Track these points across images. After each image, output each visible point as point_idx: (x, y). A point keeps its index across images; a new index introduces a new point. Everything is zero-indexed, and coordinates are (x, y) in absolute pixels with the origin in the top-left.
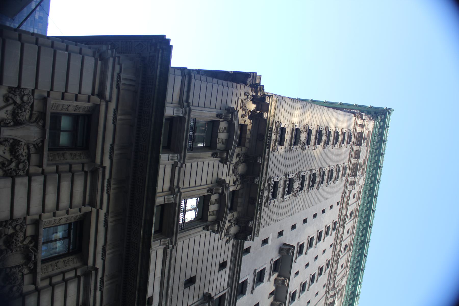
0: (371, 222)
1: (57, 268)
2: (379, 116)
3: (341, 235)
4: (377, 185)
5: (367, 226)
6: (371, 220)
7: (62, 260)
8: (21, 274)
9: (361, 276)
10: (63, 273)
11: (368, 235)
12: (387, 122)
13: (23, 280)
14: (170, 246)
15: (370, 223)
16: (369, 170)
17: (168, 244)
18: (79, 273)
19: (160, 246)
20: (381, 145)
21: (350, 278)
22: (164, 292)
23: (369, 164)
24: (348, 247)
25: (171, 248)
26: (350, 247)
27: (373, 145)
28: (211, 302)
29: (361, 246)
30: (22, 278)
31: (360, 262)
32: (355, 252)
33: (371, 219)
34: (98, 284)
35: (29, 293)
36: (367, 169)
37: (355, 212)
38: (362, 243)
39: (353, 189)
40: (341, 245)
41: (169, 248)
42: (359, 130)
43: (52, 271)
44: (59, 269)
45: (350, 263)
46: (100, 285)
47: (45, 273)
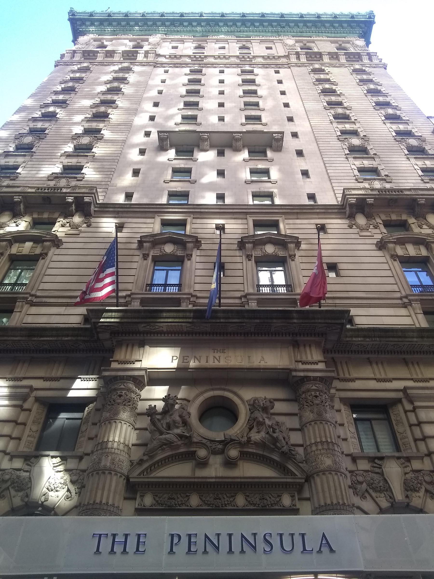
0: (216, 17)
2: (79, 28)
3: (215, 59)
4: (167, 16)
5: (221, 21)
6: (214, 16)
9: (291, 17)
11: (234, 17)
12: (85, 16)
15: (217, 17)
16: (147, 31)
20: (115, 20)
21: (294, 32)
23: (140, 33)
24: (244, 43)
26: (246, 42)
27: (115, 31)
28: (144, 240)
29: (249, 24)
31: (270, 22)
32: (256, 31)
33: (212, 16)
36: (146, 34)
37: (197, 42)
38: (246, 23)
39: (154, 52)
40: (230, 56)
42: (78, 57)
45: (271, 36)
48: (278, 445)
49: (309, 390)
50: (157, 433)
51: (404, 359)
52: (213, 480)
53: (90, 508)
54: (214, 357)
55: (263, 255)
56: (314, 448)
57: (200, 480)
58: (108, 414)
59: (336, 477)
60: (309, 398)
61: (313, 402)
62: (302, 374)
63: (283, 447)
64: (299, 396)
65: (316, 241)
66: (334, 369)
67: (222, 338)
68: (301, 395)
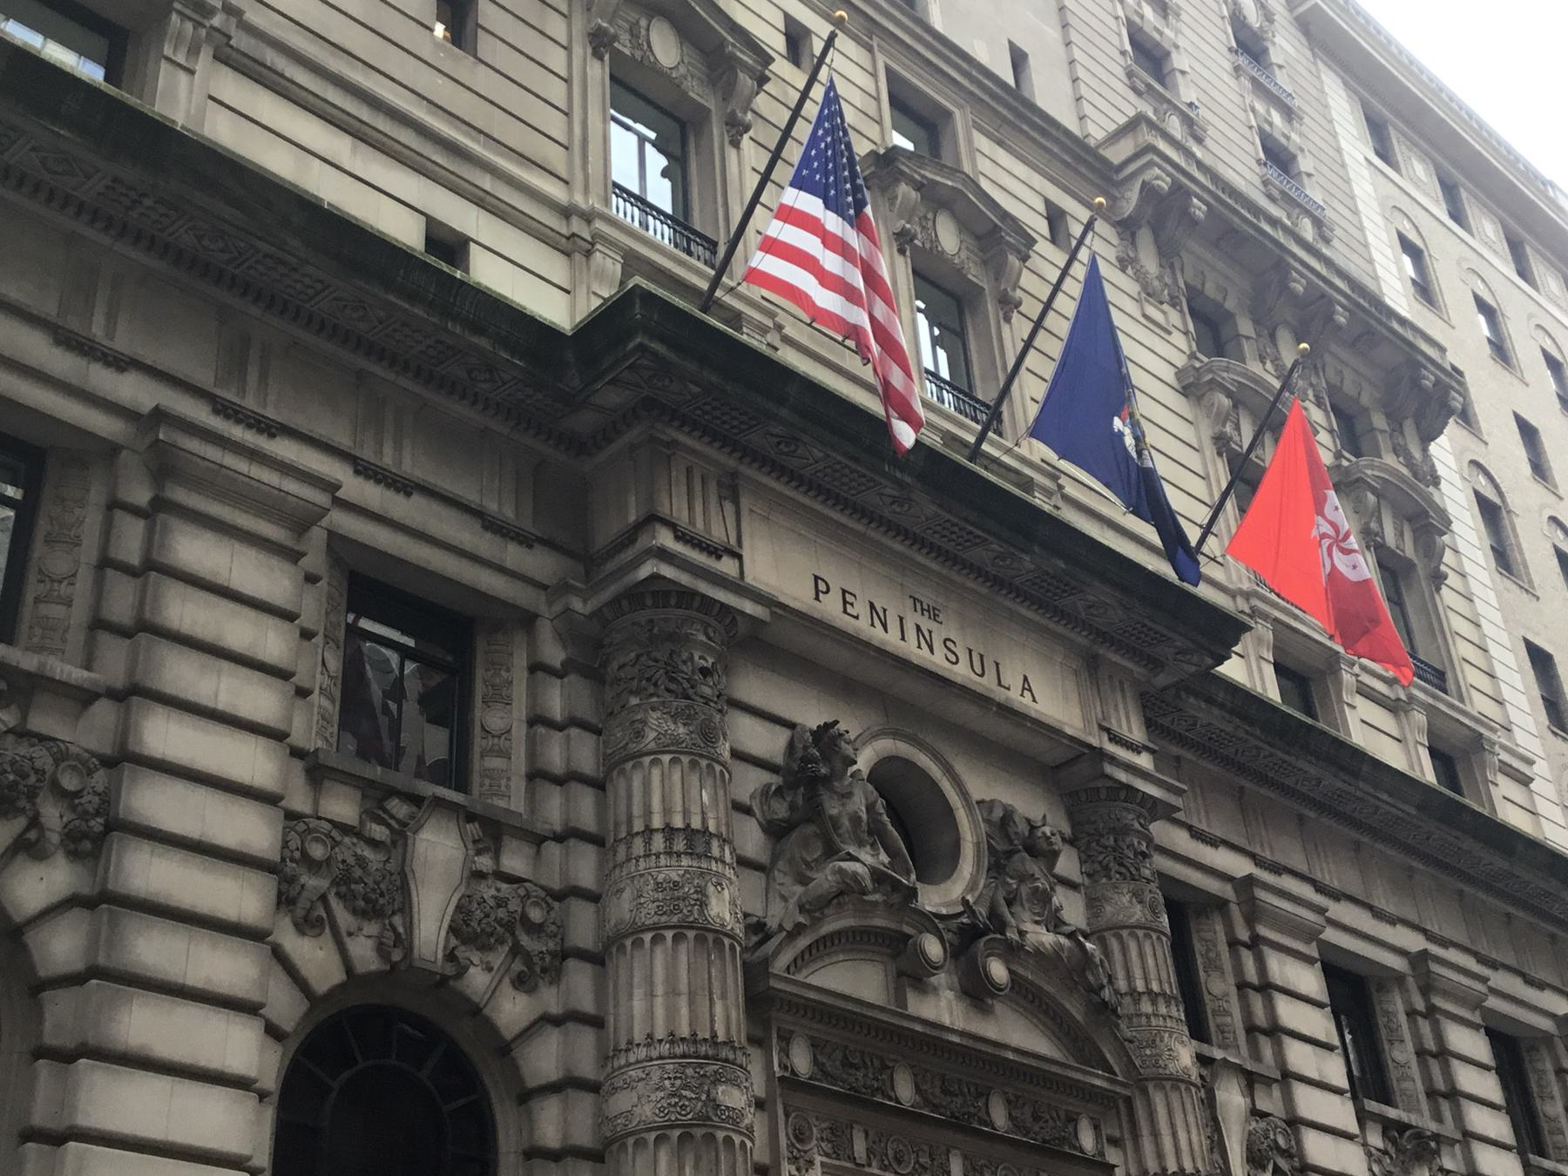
1: (66, 582)
7: (39, 549)
8: (11, 738)
10: (106, 563)
13: (43, 738)
14: (217, 21)
17: (203, 32)
18: (141, 495)
19: (191, 72)
22: (434, 158)
25: (233, 21)
30: (35, 740)
34: (238, 433)
35: (125, 730)
41: (224, 30)
43: (70, 606)
44: (74, 575)
46: (250, 426)
47: (64, 641)
48: (1091, 978)
49: (1126, 830)
50: (819, 844)
51: (1242, 789)
52: (956, 1039)
53: (710, 1053)
54: (918, 629)
55: (928, 246)
56: (1146, 1007)
57: (928, 1031)
58: (682, 730)
59: (1174, 1097)
60: (1126, 851)
61: (1138, 870)
62: (1122, 776)
63: (1102, 987)
64: (1089, 834)
65: (1054, 276)
66: (1185, 787)
67: (934, 566)
68: (1102, 836)
